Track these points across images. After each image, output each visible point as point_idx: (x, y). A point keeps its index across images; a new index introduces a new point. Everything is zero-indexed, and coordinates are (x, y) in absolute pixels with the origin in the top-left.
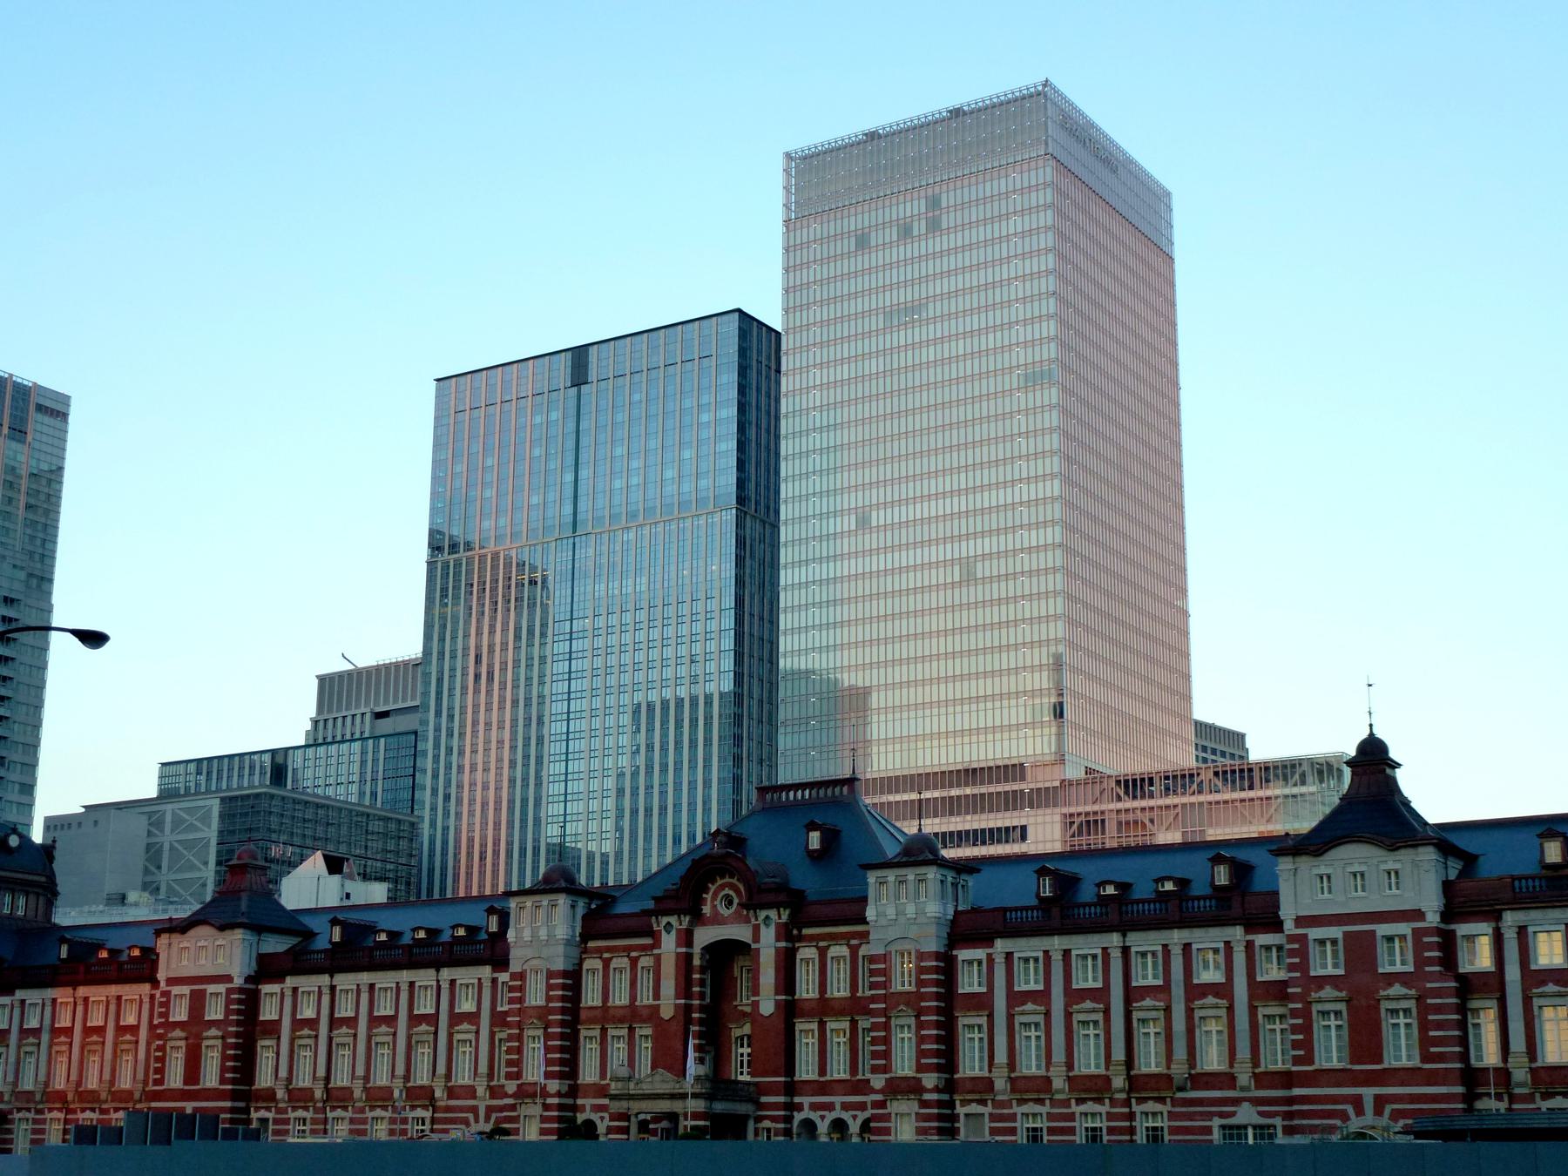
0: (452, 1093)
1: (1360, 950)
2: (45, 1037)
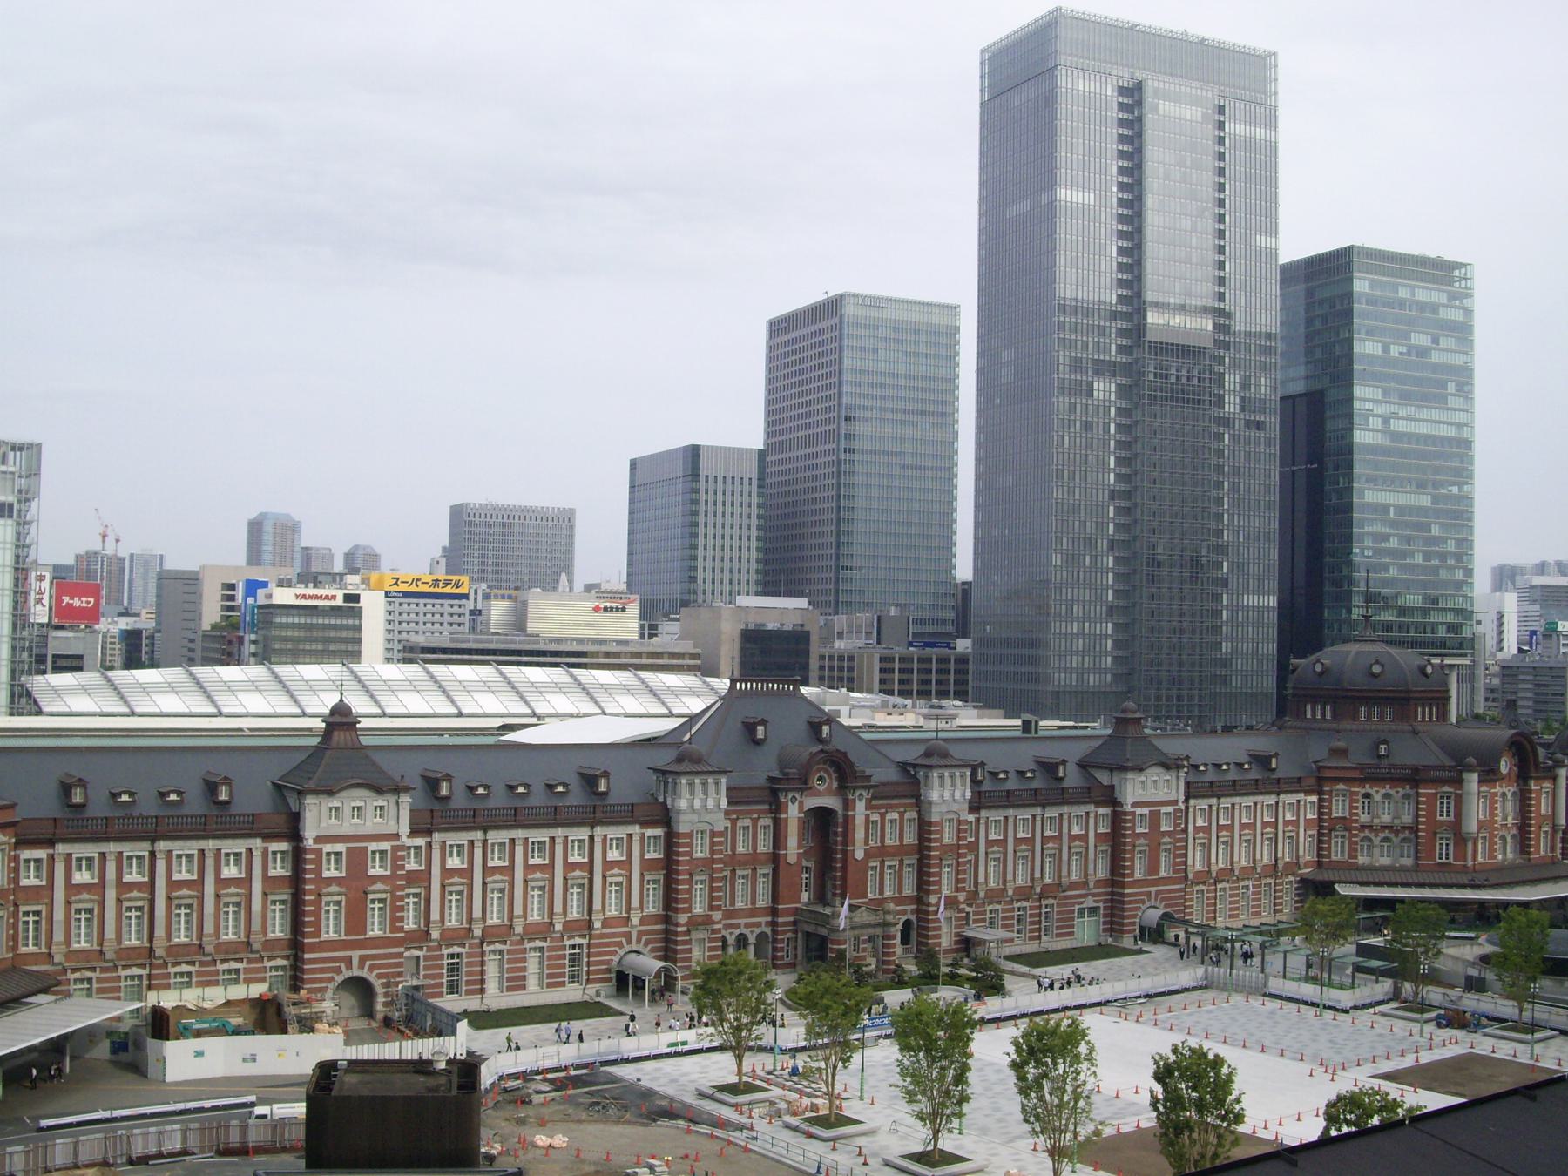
0: (606, 923)
2: (111, 894)
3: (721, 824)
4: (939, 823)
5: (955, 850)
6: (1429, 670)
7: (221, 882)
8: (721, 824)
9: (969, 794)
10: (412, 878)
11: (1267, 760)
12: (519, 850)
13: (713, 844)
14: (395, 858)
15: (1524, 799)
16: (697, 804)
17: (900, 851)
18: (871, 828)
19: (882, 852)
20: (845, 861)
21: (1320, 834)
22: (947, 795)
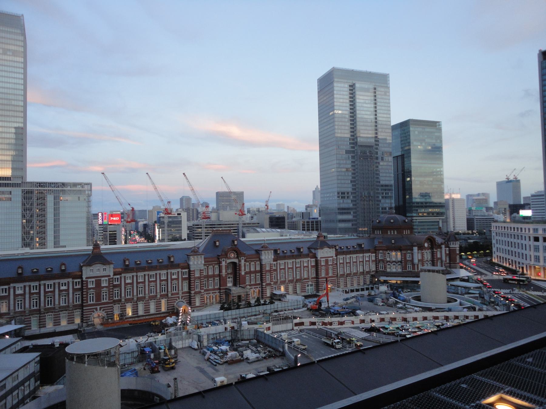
0: (172, 294)
1: (327, 261)
2: (27, 296)
3: (202, 267)
4: (265, 265)
5: (270, 271)
6: (407, 221)
7: (60, 291)
8: (202, 267)
9: (273, 257)
10: (115, 286)
11: (361, 245)
12: (147, 277)
13: (200, 273)
14: (109, 281)
15: (433, 254)
16: (196, 263)
17: (255, 272)
18: (245, 267)
19: (250, 272)
20: (239, 275)
21: (376, 264)
22: (267, 257)
